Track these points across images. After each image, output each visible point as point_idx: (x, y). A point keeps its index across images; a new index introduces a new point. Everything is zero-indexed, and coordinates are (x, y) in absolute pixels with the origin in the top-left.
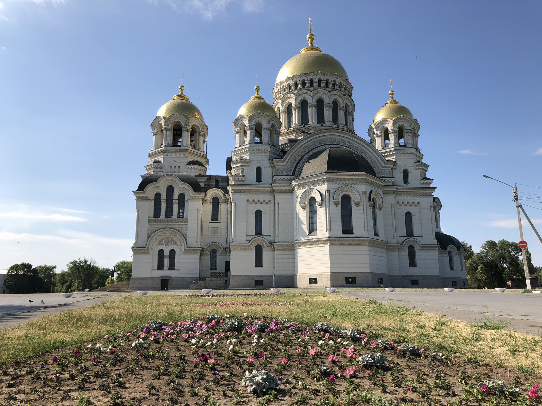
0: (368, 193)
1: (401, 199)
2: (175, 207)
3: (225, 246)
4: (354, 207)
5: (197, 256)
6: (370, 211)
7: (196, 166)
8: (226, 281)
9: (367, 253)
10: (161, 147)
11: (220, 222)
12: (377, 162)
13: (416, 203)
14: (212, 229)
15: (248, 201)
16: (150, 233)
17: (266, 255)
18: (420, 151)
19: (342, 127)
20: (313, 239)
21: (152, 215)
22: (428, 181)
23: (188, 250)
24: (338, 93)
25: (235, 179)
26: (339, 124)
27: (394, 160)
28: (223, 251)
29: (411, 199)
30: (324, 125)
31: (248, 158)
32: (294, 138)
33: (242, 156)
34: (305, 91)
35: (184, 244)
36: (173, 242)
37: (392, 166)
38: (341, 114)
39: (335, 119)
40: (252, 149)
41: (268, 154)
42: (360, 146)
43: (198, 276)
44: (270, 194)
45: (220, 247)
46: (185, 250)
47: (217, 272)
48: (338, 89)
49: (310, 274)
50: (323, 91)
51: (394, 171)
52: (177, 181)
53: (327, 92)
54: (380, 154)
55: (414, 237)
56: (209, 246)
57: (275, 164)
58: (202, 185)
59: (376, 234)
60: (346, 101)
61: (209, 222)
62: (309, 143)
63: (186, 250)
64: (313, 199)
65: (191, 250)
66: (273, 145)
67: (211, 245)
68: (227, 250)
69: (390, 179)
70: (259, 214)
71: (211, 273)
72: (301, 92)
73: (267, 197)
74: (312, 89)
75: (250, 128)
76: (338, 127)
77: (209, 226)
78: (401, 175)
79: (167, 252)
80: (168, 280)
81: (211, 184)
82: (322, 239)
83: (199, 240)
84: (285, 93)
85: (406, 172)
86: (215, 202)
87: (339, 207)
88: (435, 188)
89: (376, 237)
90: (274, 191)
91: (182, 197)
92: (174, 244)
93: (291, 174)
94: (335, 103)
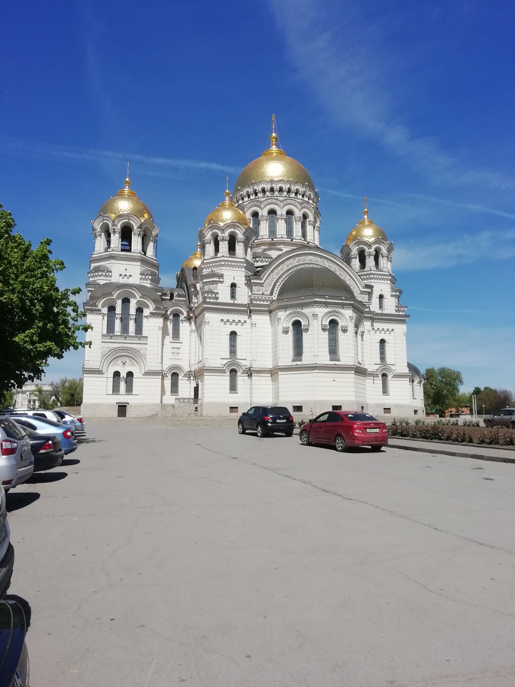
1: (377, 325)
2: (132, 325)
4: (340, 333)
9: (353, 380)
13: (390, 330)
16: (104, 353)
17: (242, 380)
20: (297, 365)
21: (105, 332)
34: (274, 201)
36: (130, 363)
47: (186, 398)
49: (294, 402)
50: (293, 202)
53: (297, 204)
57: (252, 281)
72: (269, 201)
73: (243, 318)
74: (281, 199)
79: (123, 374)
85: (381, 297)
87: (327, 333)
91: (139, 310)
93: (268, 293)
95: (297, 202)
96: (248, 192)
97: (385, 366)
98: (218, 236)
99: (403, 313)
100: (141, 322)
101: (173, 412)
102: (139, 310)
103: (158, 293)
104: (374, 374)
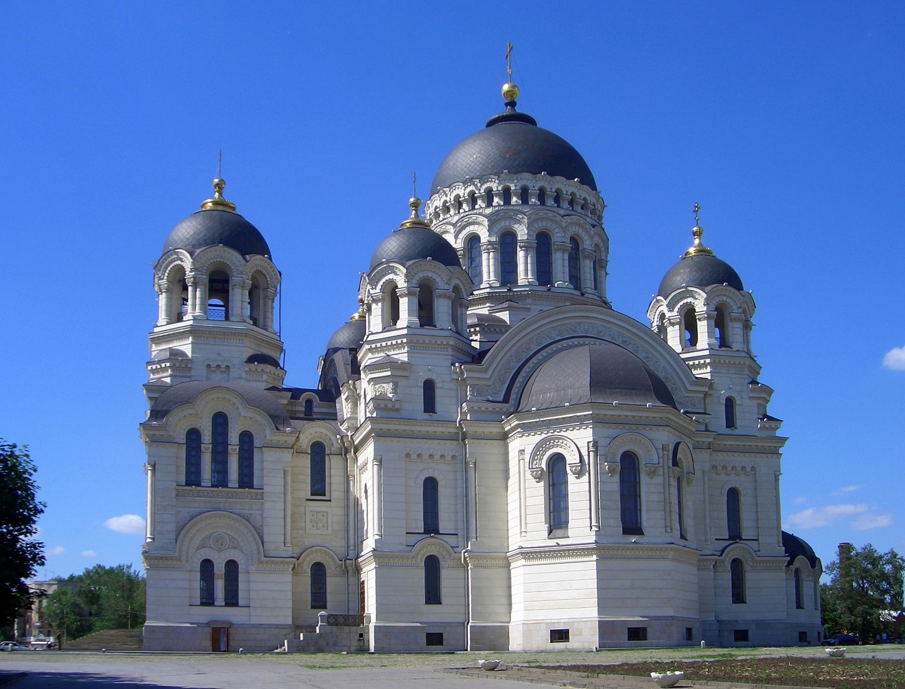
0: (671, 448)
1: (721, 458)
4: (644, 479)
11: (330, 501)
12: (677, 379)
14: (313, 515)
15: (408, 455)
18: (755, 359)
19: (590, 296)
20: (558, 545)
22: (773, 424)
25: (379, 405)
26: (583, 286)
27: (708, 376)
30: (553, 290)
31: (406, 359)
32: (487, 313)
33: (389, 354)
35: (258, 549)
37: (706, 389)
38: (587, 266)
39: (575, 279)
40: (414, 339)
41: (450, 351)
42: (643, 344)
44: (455, 443)
49: (553, 621)
50: (550, 215)
51: (708, 400)
53: (559, 218)
54: (682, 361)
59: (683, 537)
60: (597, 239)
61: (307, 500)
62: (538, 331)
64: (557, 461)
66: (457, 332)
70: (431, 486)
75: (410, 294)
76: (583, 294)
82: (575, 547)
85: (730, 403)
86: (318, 452)
87: (617, 478)
88: (784, 440)
89: (683, 542)
90: (464, 436)
92: (234, 548)
93: (501, 399)
94: (574, 240)
95: (558, 214)
96: (458, 196)
98: (397, 287)
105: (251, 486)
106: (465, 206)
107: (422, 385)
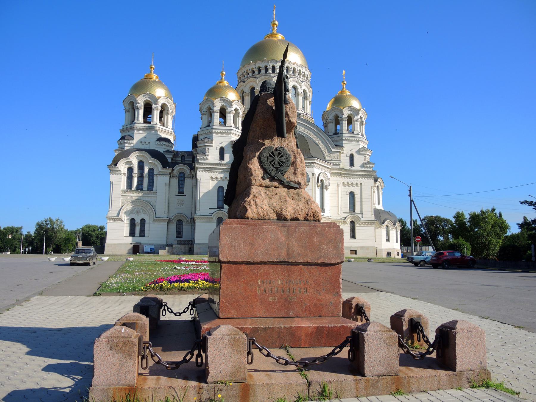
3: (190, 217)
5: (165, 225)
6: (318, 191)
7: (164, 143)
8: (190, 248)
10: (132, 124)
11: (185, 196)
14: (179, 201)
15: (212, 177)
23: (157, 219)
24: (297, 80)
28: (188, 221)
29: (355, 180)
36: (143, 212)
43: (166, 243)
45: (185, 218)
46: (154, 219)
48: (297, 76)
52: (147, 157)
55: (356, 213)
56: (175, 217)
58: (170, 160)
61: (176, 195)
63: (155, 219)
65: (159, 220)
67: (177, 215)
68: (192, 221)
69: (338, 163)
71: (178, 241)
74: (273, 75)
77: (176, 199)
78: (348, 159)
79: (138, 221)
80: (139, 245)
81: (178, 159)
83: (167, 211)
84: (248, 76)
92: (144, 214)
97: (352, 214)
99: (371, 169)
100: (153, 179)
101: (171, 251)
102: (151, 170)
103: (166, 156)
104: (341, 221)
105: (152, 190)
106: (250, 74)
107: (219, 149)
